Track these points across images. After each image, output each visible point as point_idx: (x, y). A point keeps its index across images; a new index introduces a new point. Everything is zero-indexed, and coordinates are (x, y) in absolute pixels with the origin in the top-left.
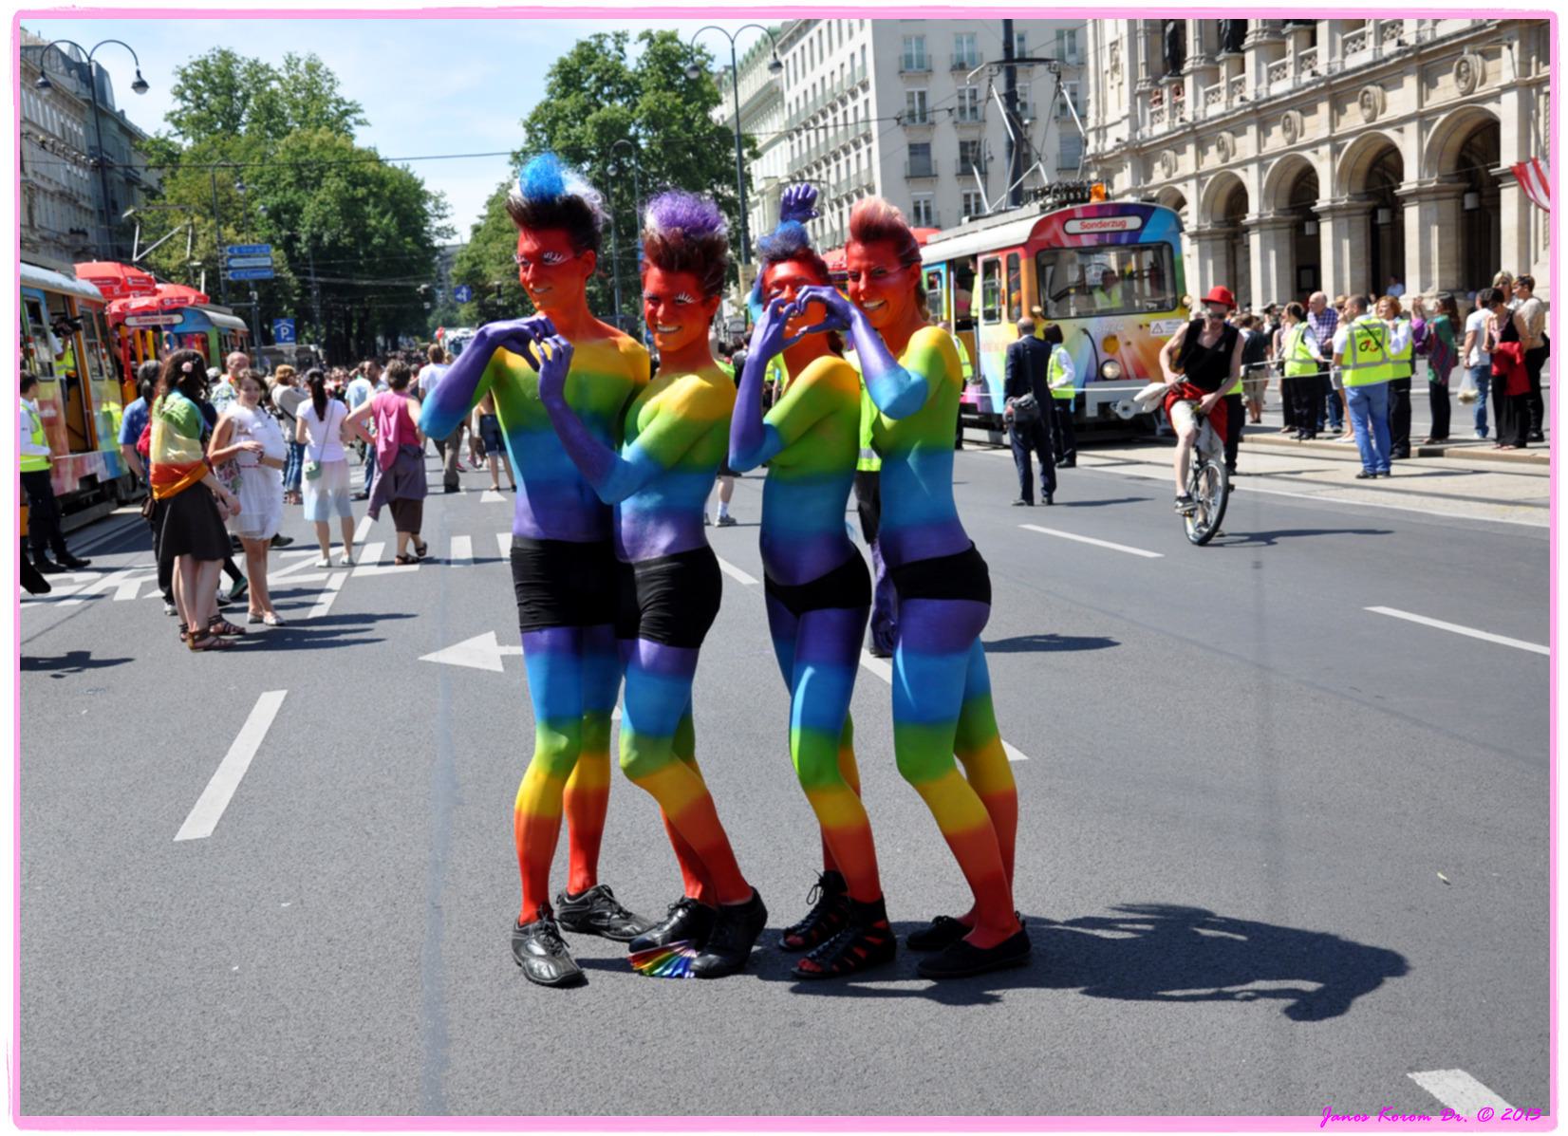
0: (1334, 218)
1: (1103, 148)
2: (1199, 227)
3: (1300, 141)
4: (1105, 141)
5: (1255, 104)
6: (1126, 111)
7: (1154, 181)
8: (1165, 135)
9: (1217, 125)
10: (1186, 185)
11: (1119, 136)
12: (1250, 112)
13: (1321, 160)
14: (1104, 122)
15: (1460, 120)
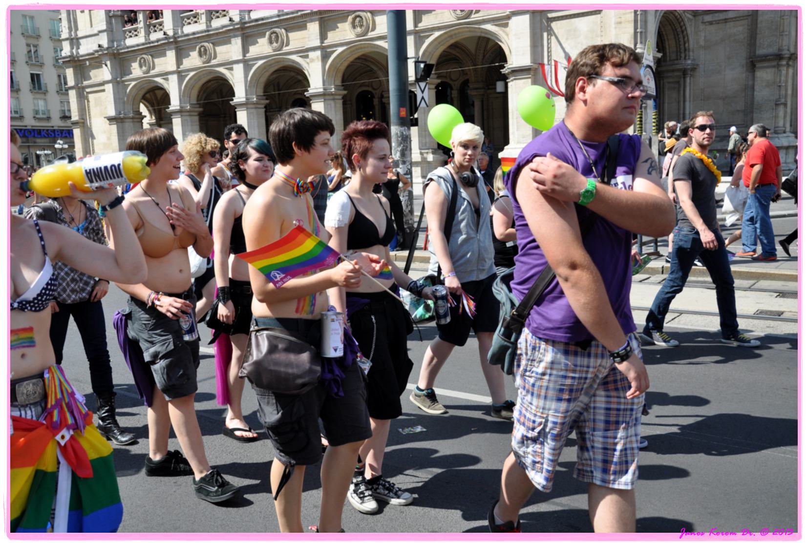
0: (324, 101)
1: (78, 53)
2: (181, 107)
3: (286, 49)
4: (78, 48)
5: (242, 23)
6: (104, 26)
7: (131, 76)
8: (143, 44)
9: (198, 37)
10: (167, 79)
11: (100, 43)
12: (238, 29)
13: (312, 61)
14: (77, 35)
15: (451, 36)
